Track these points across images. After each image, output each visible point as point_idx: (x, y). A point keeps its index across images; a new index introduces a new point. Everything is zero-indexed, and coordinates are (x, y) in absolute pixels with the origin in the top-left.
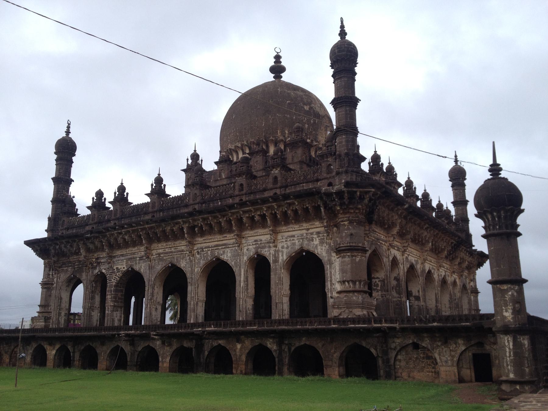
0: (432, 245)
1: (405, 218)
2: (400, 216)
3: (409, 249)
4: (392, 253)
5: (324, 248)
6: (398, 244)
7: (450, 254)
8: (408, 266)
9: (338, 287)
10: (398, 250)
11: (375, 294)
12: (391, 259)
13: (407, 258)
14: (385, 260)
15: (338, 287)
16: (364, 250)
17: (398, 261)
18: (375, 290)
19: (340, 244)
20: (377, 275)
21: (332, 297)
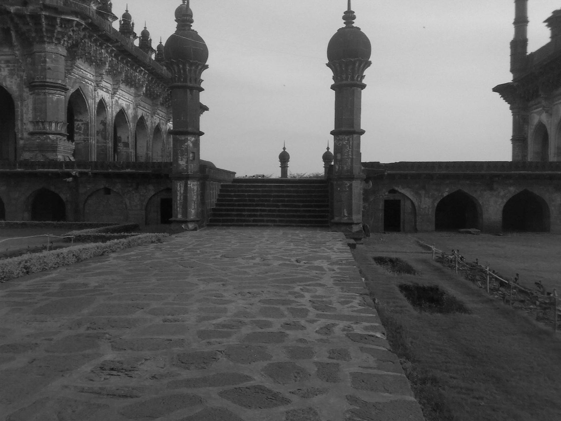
0: (146, 90)
1: (116, 56)
2: (110, 54)
3: (120, 91)
4: (100, 94)
5: (14, 80)
6: (109, 85)
7: (166, 101)
8: (118, 110)
9: (30, 128)
10: (107, 92)
11: (76, 137)
12: (98, 100)
13: (117, 101)
14: (90, 101)
15: (30, 128)
16: (64, 89)
17: (106, 104)
18: (77, 133)
19: (34, 79)
20: (80, 117)
21: (22, 139)
